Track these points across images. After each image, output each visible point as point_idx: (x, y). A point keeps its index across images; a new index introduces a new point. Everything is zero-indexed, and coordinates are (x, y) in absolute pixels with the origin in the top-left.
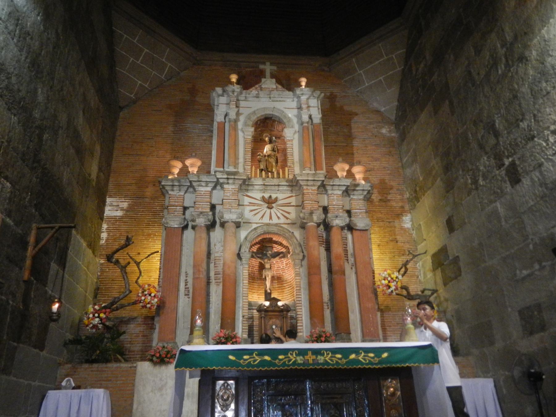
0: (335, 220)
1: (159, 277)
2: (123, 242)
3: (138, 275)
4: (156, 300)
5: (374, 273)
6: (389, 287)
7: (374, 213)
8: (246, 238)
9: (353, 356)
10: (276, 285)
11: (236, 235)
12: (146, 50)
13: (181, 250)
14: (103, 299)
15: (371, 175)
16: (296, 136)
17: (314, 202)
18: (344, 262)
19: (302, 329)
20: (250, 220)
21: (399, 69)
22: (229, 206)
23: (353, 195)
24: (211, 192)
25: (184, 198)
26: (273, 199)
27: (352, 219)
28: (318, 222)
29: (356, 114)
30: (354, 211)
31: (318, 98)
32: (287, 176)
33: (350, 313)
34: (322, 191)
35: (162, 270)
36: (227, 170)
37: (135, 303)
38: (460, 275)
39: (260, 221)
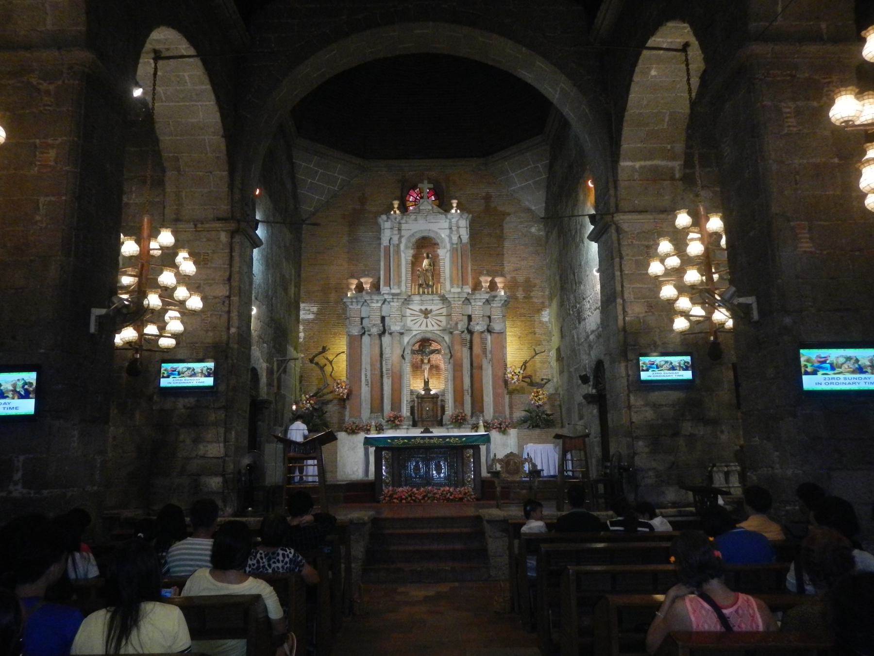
1: (347, 371)
2: (320, 349)
3: (331, 370)
4: (346, 391)
5: (506, 366)
6: (513, 379)
7: (518, 309)
8: (408, 343)
9: (448, 440)
10: (434, 372)
11: (400, 342)
12: (320, 171)
13: (361, 352)
16: (448, 255)
18: (481, 360)
19: (449, 409)
20: (411, 328)
23: (493, 303)
24: (381, 307)
25: (361, 311)
26: (429, 310)
27: (491, 324)
29: (509, 214)
31: (467, 218)
32: (439, 293)
33: (484, 396)
35: (348, 367)
36: (393, 291)
37: (331, 392)
38: (563, 372)
39: (419, 329)
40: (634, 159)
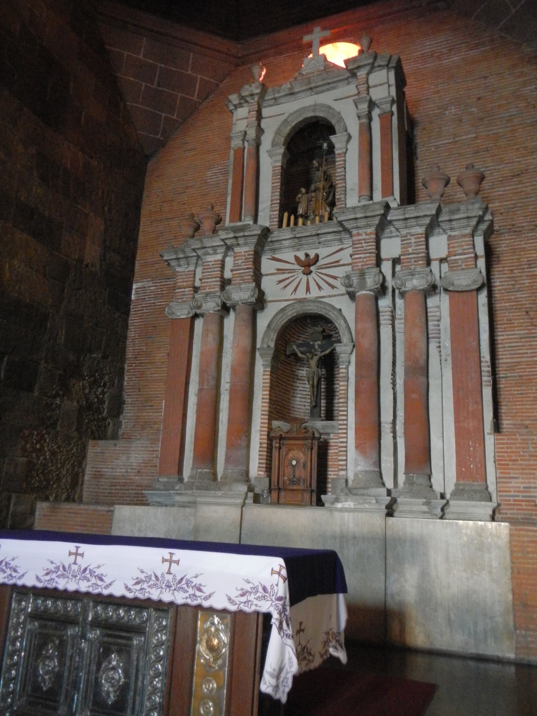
0: (412, 279)
7: (522, 253)
14: (130, 414)
15: (520, 182)
17: (368, 255)
22: (240, 280)
23: (452, 229)
28: (372, 288)
30: (453, 258)
34: (391, 232)
39: (293, 297)
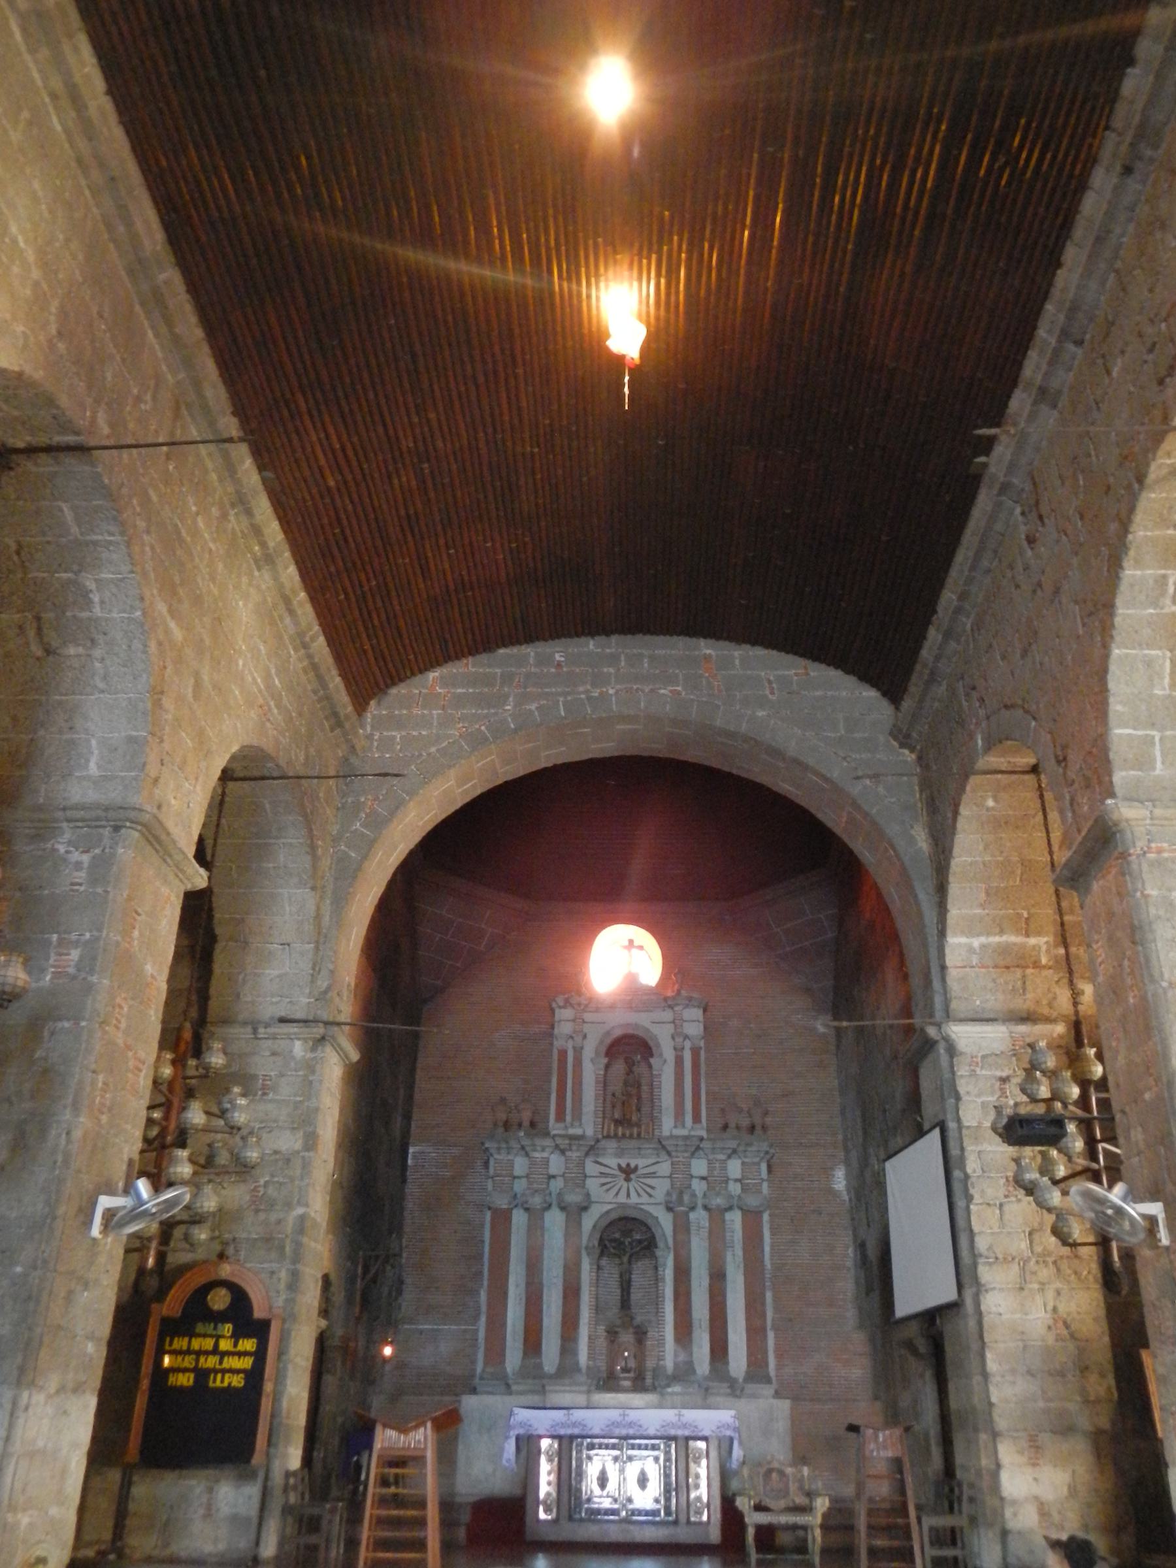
21: (830, 935)
36: (571, 1131)
40: (970, 932)
